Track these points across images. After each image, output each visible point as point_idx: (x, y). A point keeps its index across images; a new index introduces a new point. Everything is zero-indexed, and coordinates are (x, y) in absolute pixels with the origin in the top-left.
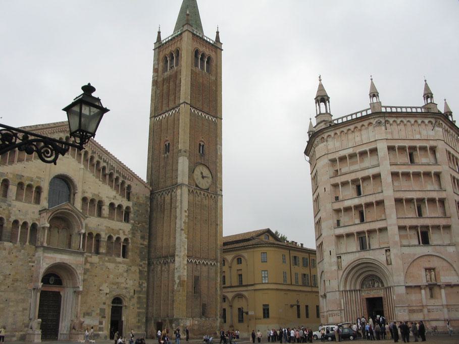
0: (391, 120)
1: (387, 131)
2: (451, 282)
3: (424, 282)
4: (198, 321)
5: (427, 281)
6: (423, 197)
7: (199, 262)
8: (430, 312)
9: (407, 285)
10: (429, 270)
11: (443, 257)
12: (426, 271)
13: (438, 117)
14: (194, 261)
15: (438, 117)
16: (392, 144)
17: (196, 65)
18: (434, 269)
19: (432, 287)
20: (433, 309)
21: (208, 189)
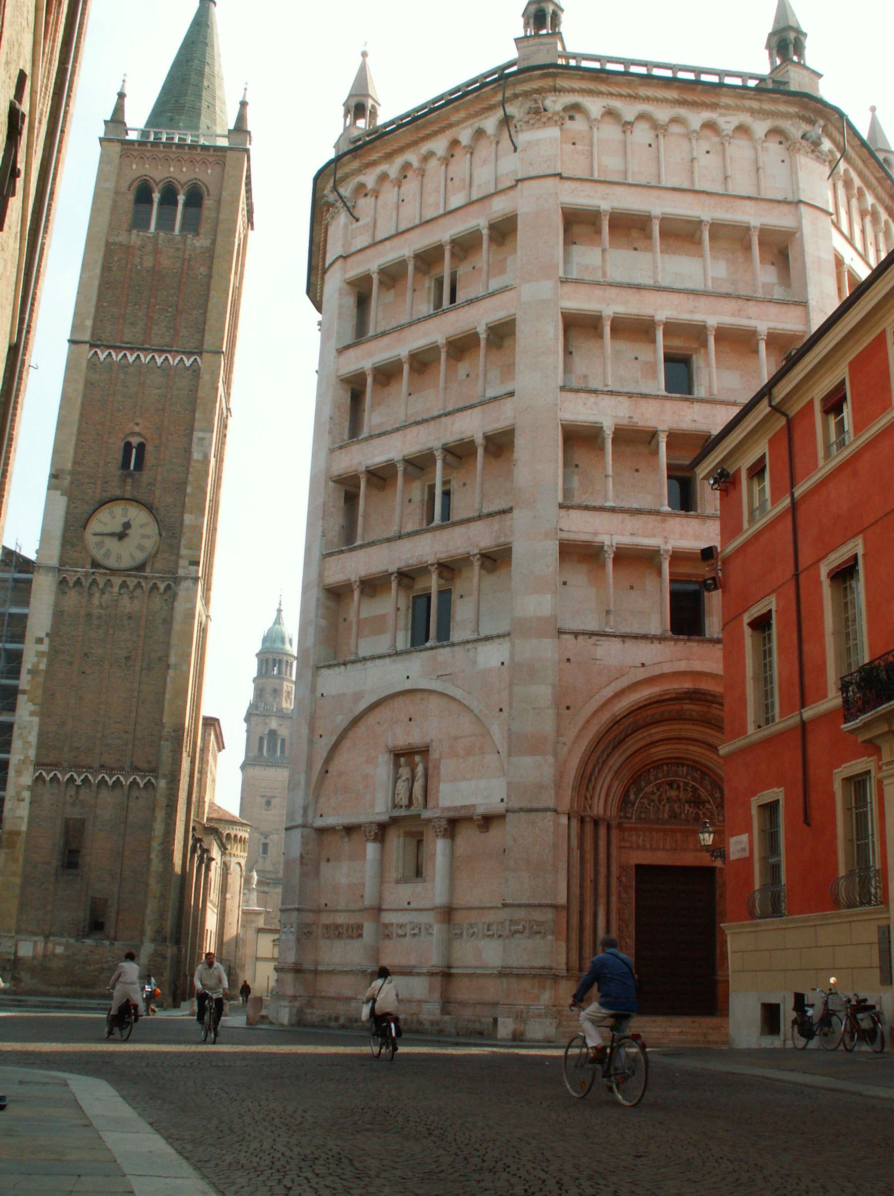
0: (369, 179)
1: (359, 223)
2: (474, 806)
3: (377, 810)
4: (67, 946)
5: (395, 806)
6: (429, 445)
7: (86, 780)
8: (388, 936)
9: (319, 823)
10: (403, 756)
11: (458, 694)
12: (397, 766)
13: (536, 85)
14: (63, 778)
15: (536, 85)
16: (355, 270)
17: (140, 222)
18: (424, 751)
19: (406, 829)
20: (401, 926)
21: (141, 568)
